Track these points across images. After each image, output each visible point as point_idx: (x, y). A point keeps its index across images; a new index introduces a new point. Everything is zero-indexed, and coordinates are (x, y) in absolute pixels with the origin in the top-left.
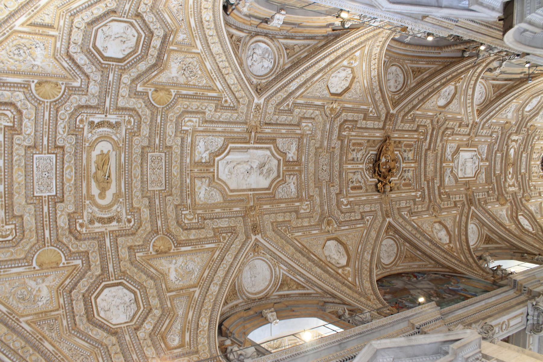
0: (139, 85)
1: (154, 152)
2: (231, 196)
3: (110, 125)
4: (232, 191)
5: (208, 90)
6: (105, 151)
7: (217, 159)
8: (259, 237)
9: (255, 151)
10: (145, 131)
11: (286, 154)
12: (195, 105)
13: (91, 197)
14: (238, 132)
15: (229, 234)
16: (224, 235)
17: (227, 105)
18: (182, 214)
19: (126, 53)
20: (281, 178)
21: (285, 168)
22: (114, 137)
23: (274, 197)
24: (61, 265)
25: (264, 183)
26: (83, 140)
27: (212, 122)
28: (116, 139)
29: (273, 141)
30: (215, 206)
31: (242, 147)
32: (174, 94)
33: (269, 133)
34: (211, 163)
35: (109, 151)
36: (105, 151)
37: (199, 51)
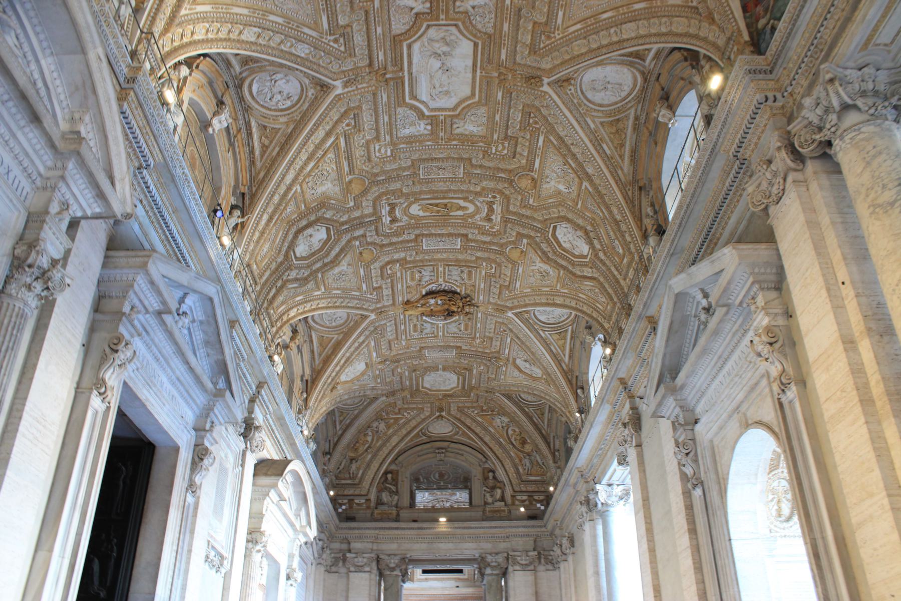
0: (348, 206)
2: (480, 97)
3: (392, 211)
4: (473, 94)
5: (338, 150)
7: (427, 113)
8: (546, 80)
9: (414, 66)
11: (417, 14)
12: (358, 153)
13: (464, 218)
14: (388, 97)
15: (532, 115)
16: (531, 121)
17: (353, 122)
18: (495, 154)
19: (319, 228)
20: (460, 24)
21: (442, 17)
23: (490, 36)
25: (465, 47)
26: (410, 224)
27: (377, 130)
28: (406, 204)
29: (396, 41)
30: (491, 118)
31: (409, 84)
32: (350, 177)
33: (385, 54)
34: (433, 121)
37: (298, 187)
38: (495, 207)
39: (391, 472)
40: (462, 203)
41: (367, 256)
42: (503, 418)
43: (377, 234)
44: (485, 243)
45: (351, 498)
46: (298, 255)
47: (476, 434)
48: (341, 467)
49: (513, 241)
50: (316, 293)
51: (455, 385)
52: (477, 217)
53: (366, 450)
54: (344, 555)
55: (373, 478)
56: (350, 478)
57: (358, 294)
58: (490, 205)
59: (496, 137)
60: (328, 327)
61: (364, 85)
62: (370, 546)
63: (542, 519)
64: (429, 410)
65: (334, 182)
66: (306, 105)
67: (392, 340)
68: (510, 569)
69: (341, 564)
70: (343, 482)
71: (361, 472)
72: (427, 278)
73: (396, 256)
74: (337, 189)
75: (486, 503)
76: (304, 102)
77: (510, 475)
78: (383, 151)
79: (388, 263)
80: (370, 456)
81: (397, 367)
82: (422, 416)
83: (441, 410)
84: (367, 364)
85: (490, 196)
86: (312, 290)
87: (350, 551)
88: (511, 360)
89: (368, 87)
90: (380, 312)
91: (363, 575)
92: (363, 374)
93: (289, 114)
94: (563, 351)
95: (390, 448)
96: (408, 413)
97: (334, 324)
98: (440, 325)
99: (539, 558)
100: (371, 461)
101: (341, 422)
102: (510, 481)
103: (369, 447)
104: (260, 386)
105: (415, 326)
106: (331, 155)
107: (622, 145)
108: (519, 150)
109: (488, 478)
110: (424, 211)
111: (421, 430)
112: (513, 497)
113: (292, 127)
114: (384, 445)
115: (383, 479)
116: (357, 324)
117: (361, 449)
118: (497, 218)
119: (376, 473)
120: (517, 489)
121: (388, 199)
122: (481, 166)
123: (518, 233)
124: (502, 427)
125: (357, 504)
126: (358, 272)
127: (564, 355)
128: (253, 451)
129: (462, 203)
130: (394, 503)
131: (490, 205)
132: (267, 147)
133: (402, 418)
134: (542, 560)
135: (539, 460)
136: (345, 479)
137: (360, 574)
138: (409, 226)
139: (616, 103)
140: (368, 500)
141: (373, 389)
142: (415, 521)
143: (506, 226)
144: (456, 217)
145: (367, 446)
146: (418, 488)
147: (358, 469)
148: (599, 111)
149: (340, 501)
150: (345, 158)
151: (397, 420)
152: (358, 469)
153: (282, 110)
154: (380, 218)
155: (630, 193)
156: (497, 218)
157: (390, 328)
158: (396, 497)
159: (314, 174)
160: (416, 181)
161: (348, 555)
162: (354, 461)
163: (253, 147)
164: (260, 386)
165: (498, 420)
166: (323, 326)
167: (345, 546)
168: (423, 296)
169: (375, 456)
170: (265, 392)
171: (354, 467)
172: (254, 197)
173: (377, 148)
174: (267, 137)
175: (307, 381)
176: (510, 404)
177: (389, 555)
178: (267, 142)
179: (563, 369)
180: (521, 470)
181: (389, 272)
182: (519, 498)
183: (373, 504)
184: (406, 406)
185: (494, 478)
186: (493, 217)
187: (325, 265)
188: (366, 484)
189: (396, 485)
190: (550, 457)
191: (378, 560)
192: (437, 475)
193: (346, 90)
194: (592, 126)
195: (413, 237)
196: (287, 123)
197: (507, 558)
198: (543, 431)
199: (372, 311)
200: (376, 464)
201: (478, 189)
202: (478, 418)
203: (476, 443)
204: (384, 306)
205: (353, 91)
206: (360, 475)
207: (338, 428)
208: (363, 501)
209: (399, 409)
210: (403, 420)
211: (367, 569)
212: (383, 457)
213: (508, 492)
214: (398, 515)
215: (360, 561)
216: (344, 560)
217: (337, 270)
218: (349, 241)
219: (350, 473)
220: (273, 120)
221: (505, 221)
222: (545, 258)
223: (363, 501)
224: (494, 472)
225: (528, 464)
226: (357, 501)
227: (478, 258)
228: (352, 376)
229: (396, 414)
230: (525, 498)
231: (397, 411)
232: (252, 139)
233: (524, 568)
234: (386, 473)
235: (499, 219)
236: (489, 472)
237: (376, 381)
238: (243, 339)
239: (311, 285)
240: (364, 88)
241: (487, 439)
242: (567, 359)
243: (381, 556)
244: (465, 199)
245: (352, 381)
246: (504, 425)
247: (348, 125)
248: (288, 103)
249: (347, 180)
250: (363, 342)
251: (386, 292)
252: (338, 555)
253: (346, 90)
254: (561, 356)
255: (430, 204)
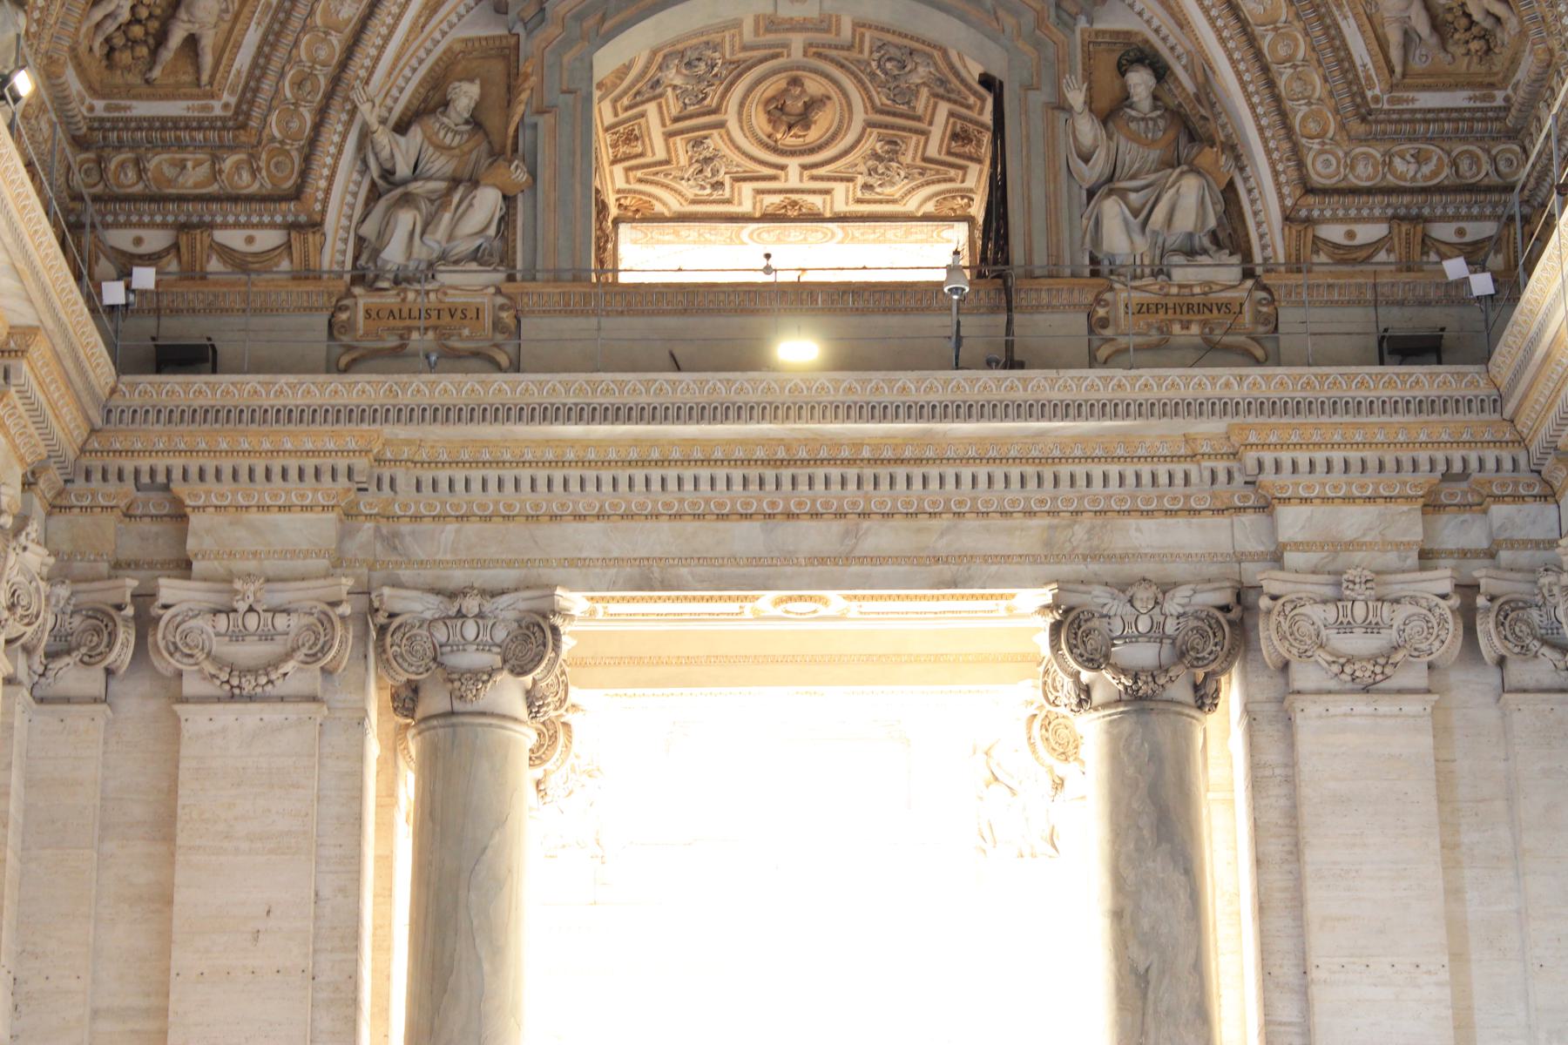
45: (192, 211)
54: (144, 597)
63: (1484, 358)
87: (184, 567)
91: (272, 714)
99: (1468, 615)
109: (1125, 99)
120: (1322, 171)
137: (251, 715)
149: (121, 239)
161: (170, 589)
182: (1334, 233)
208: (268, 239)
211: (296, 676)
230: (1368, 233)
236: (1122, 70)
243: (391, 598)
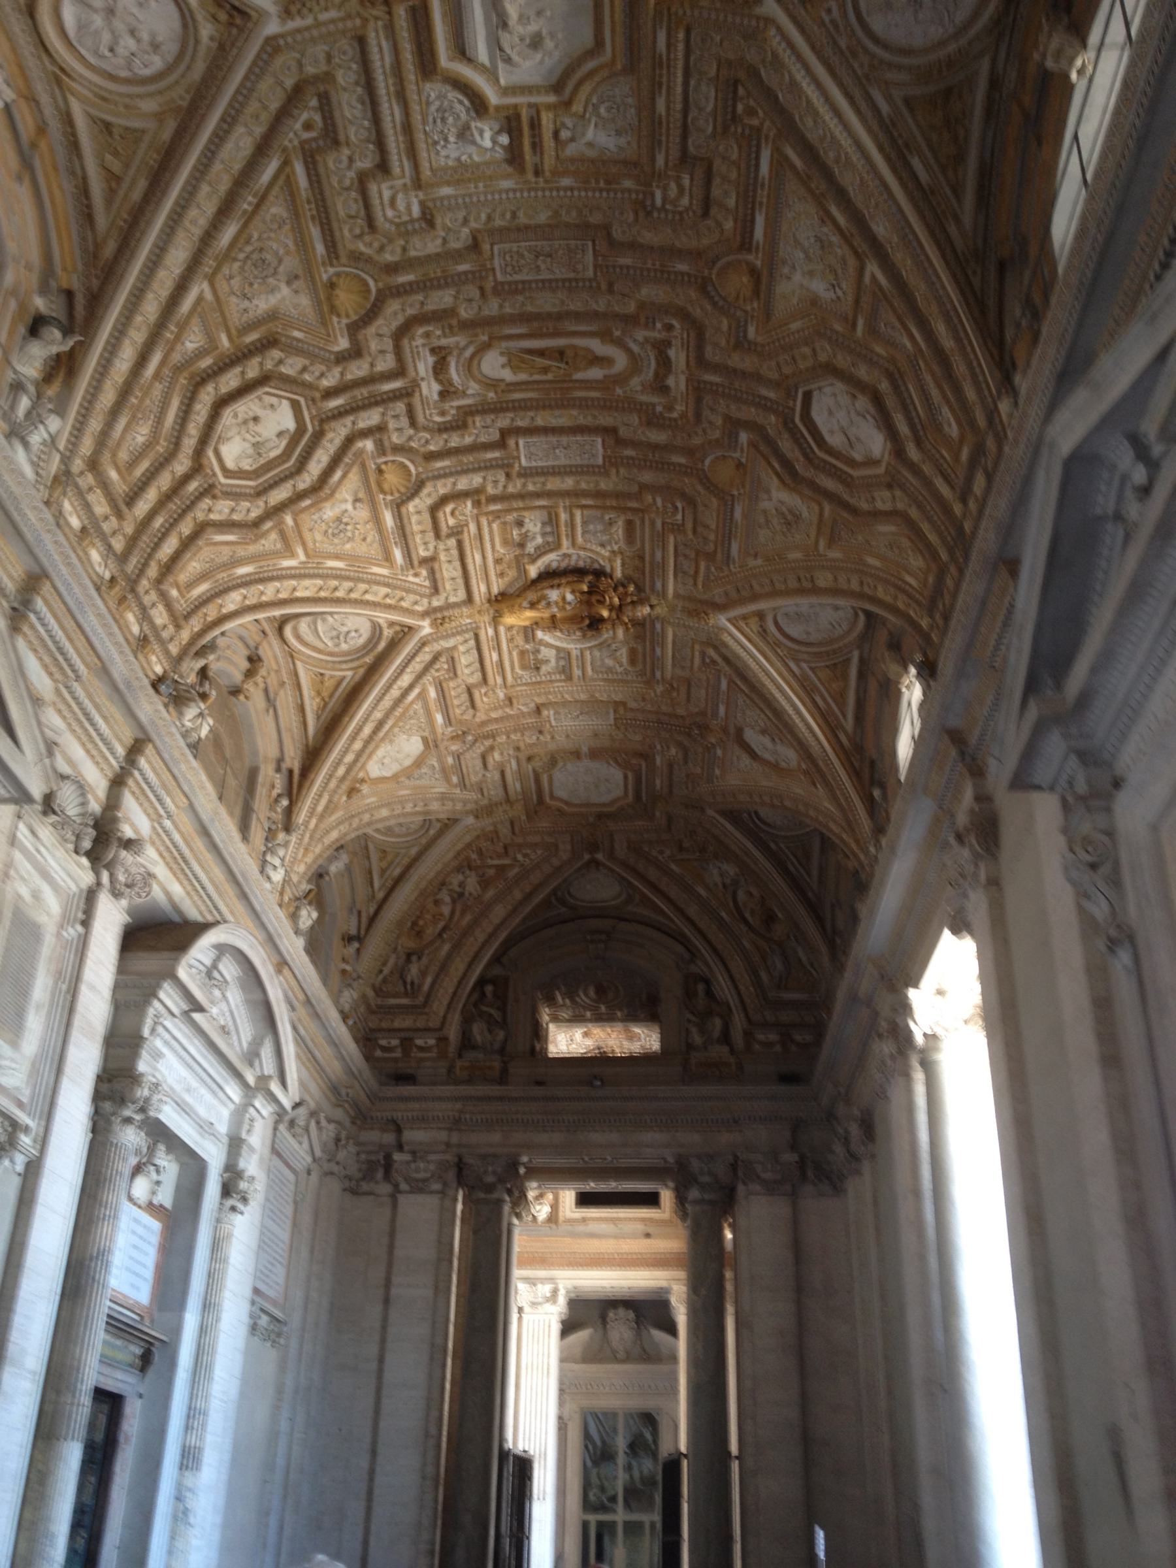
0: (336, 349)
1: (493, 269)
3: (439, 369)
4: (599, 43)
6: (503, 360)
10: (443, 299)
12: (344, 206)
13: (607, 384)
15: (741, 91)
16: (740, 108)
17: (318, 118)
19: (274, 400)
22: (468, 353)
24: (744, 460)
32: (331, 270)
35: (502, 354)
36: (503, 360)
37: (205, 286)
38: (672, 353)
39: (493, 981)
40: (596, 346)
41: (392, 478)
42: (725, 867)
43: (413, 423)
44: (655, 447)
46: (230, 464)
47: (670, 901)
48: (386, 971)
49: (717, 441)
50: (287, 563)
51: (619, 792)
52: (635, 382)
53: (440, 935)
54: (388, 1157)
55: (455, 994)
56: (406, 994)
57: (384, 571)
58: (661, 348)
59: (660, 161)
60: (331, 654)
61: (333, 14)
62: (443, 1136)
64: (569, 847)
65: (297, 284)
66: (200, 67)
67: (476, 686)
68: (741, 1189)
69: (380, 1175)
70: (392, 1001)
71: (429, 980)
72: (539, 540)
73: (463, 483)
74: (305, 301)
75: (690, 1047)
76: (193, 59)
77: (741, 987)
78: (401, 204)
79: (444, 500)
80: (446, 948)
81: (492, 748)
82: (555, 862)
83: (594, 847)
84: (425, 740)
85: (659, 325)
86: (276, 554)
87: (400, 1147)
88: (732, 730)
89: (342, 19)
90: (438, 616)
92: (419, 762)
93: (160, 92)
94: (842, 706)
95: (490, 929)
96: (525, 855)
97: (344, 647)
98: (574, 653)
100: (449, 957)
101: (383, 871)
102: (742, 1001)
103: (444, 929)
104: (135, 749)
105: (522, 653)
106: (276, 209)
107: (959, 158)
108: (716, 192)
110: (515, 369)
111: (554, 892)
112: (748, 1035)
113: (171, 126)
114: (475, 923)
115: (476, 995)
116: (394, 645)
117: (430, 932)
118: (678, 382)
119: (460, 982)
121: (427, 335)
122: (633, 246)
123: (727, 418)
124: (724, 886)
125: (421, 1049)
126: (377, 520)
127: (844, 716)
128: (116, 894)
129: (596, 346)
130: (497, 1046)
131: (661, 348)
132: (118, 179)
133: (511, 866)
134: (810, 1174)
135: (804, 959)
136: (396, 995)
138: (484, 409)
139: (942, 43)
140: (443, 1040)
141: (443, 798)
142: (539, 1083)
143: (699, 401)
144: (587, 384)
145: (441, 925)
146: (555, 1019)
147: (423, 974)
148: (899, 67)
150: (313, 218)
151: (501, 869)
152: (423, 974)
153: (144, 81)
154: (415, 385)
155: (976, 282)
156: (678, 382)
157: (466, 660)
158: (501, 1035)
159: (241, 256)
160: (489, 285)
161: (397, 1156)
162: (414, 958)
163: (85, 179)
164: (135, 749)
165: (715, 871)
166: (319, 651)
167: (389, 1138)
168: (534, 582)
169: (457, 946)
170: (149, 762)
171: (414, 970)
172: (97, 301)
173: (387, 194)
174: (115, 154)
175: (291, 772)
176: (738, 835)
177: (484, 1157)
178: (116, 166)
179: (842, 746)
180: (764, 975)
181: (451, 521)
182: (761, 1037)
183: (452, 1049)
184: (519, 840)
185: (709, 993)
186: (671, 381)
187: (299, 496)
188: (439, 1006)
189: (503, 1009)
190: (824, 949)
191: (460, 1167)
192: (592, 993)
193: (291, 25)
194: (885, 108)
195: (495, 436)
196: (159, 117)
197: (734, 1167)
198: (810, 894)
199: (425, 614)
200: (458, 966)
201: (631, 308)
202: (673, 867)
203: (668, 917)
204: (449, 606)
205: (308, 29)
206: (426, 987)
207: (377, 884)
208: (432, 1042)
209: (505, 848)
210: (516, 870)
211: (436, 1186)
212: (475, 949)
213: (738, 1022)
214: (504, 1071)
215: (422, 1169)
216: (388, 1166)
217: (329, 512)
218: (349, 441)
219: (405, 983)
220: (127, 106)
221: (698, 390)
222: (791, 476)
223: (432, 1042)
224: (707, 982)
225: (779, 965)
226: (419, 1042)
227: (643, 487)
228: (395, 768)
229: (499, 856)
231: (500, 849)
232: (80, 157)
233: (771, 1188)
234: (481, 982)
235: (683, 386)
237: (447, 780)
238: (70, 624)
239: (271, 541)
240: (333, 21)
241: (692, 910)
242: (849, 724)
244: (605, 336)
245: (395, 777)
246: (728, 881)
247: (308, 126)
248: (157, 63)
249: (325, 277)
250: (411, 687)
251: (449, 571)
252: (373, 1158)
253: (291, 25)
254: (837, 719)
255: (530, 352)
